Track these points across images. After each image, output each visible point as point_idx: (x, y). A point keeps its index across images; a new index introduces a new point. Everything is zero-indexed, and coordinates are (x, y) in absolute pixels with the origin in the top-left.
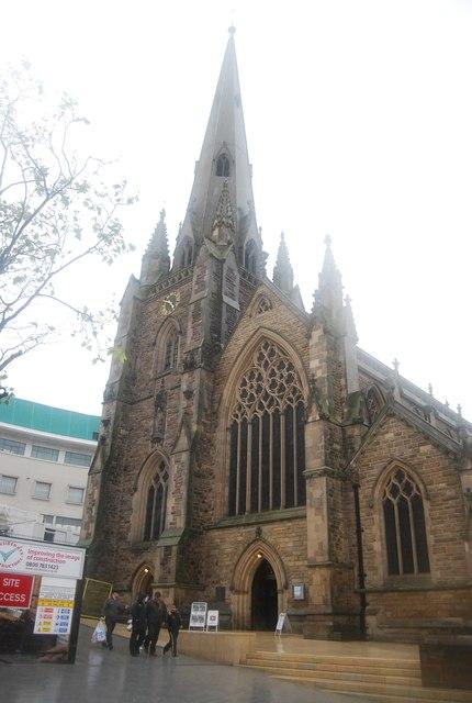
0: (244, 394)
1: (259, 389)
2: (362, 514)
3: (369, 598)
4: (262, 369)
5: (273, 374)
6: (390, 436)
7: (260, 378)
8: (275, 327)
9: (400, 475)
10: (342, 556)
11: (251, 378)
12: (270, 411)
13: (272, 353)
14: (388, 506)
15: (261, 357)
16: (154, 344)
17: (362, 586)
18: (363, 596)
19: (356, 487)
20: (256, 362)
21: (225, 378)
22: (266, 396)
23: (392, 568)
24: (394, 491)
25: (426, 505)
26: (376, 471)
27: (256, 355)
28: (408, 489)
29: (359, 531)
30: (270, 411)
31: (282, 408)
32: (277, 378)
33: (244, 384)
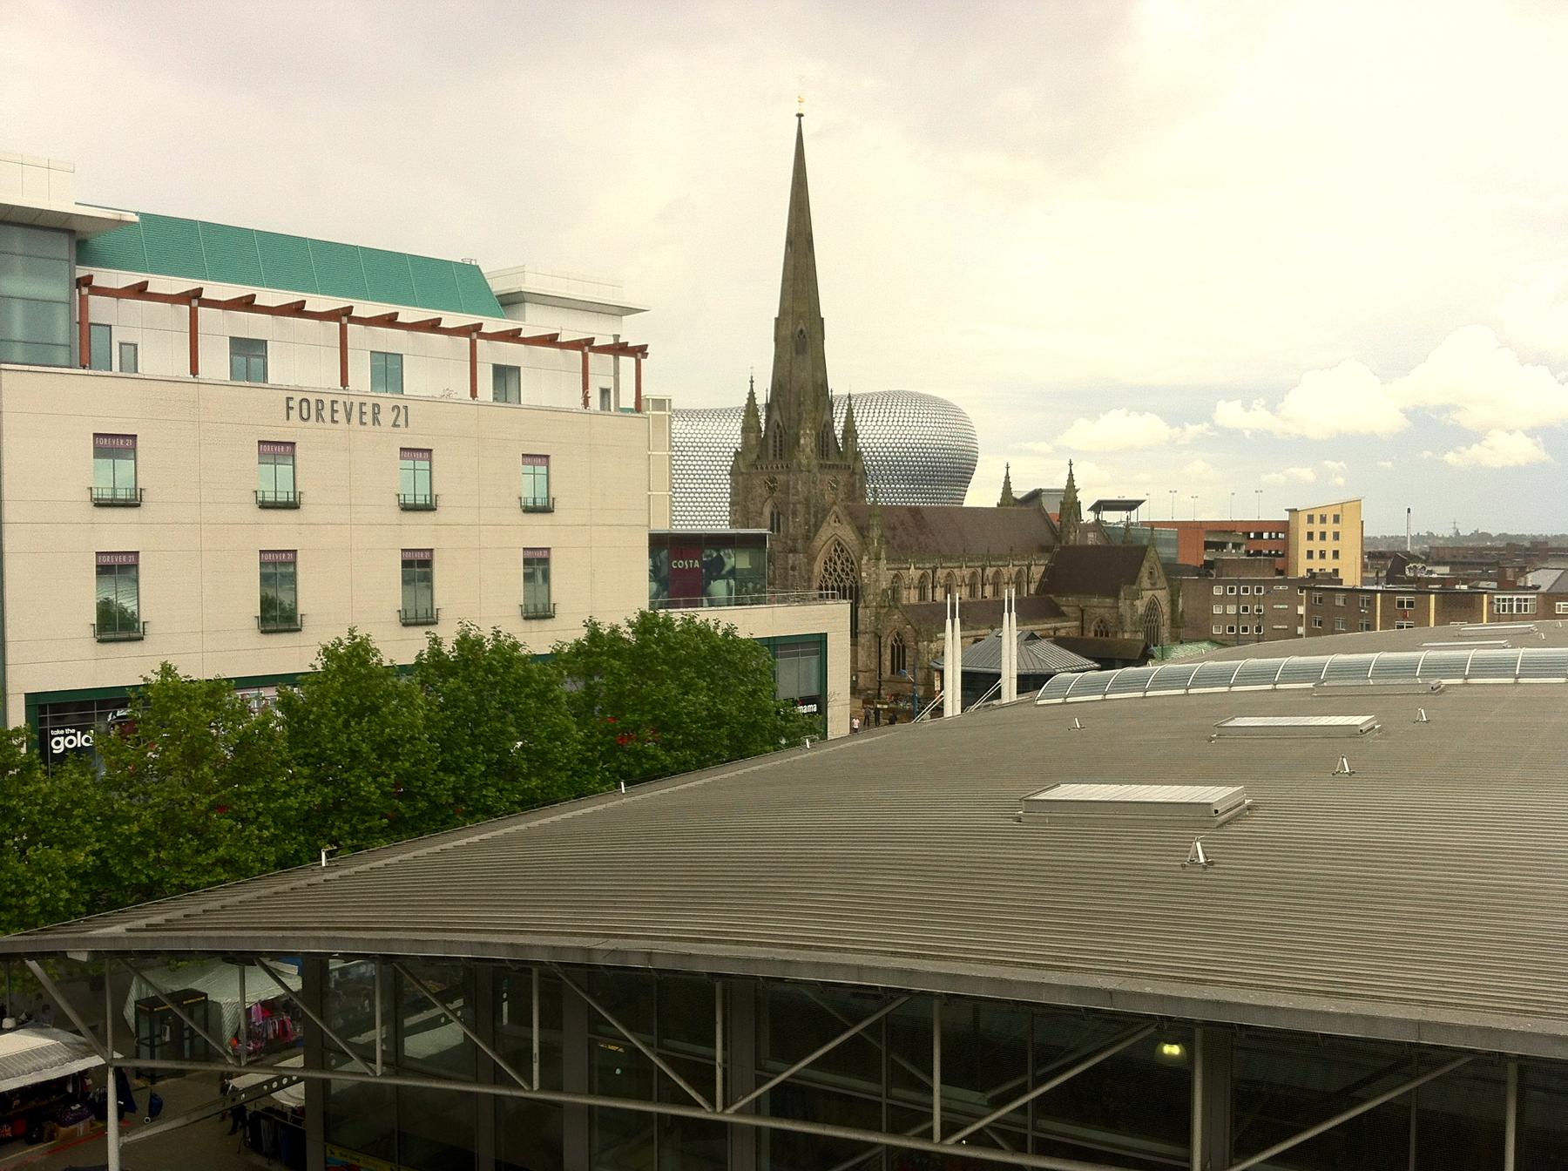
0: (826, 570)
1: (835, 570)
2: (882, 649)
3: (882, 683)
4: (836, 558)
5: (842, 563)
6: (896, 617)
7: (835, 563)
8: (843, 537)
9: (898, 634)
10: (872, 667)
11: (830, 560)
12: (841, 585)
13: (842, 551)
14: (893, 646)
15: (836, 550)
16: (762, 514)
17: (880, 678)
18: (880, 682)
19: (880, 637)
20: (833, 553)
21: (815, 559)
22: (839, 576)
23: (893, 672)
24: (896, 641)
25: (907, 650)
26: (888, 631)
27: (833, 549)
28: (901, 641)
29: (880, 656)
30: (841, 585)
31: (848, 586)
32: (845, 567)
33: (826, 563)
